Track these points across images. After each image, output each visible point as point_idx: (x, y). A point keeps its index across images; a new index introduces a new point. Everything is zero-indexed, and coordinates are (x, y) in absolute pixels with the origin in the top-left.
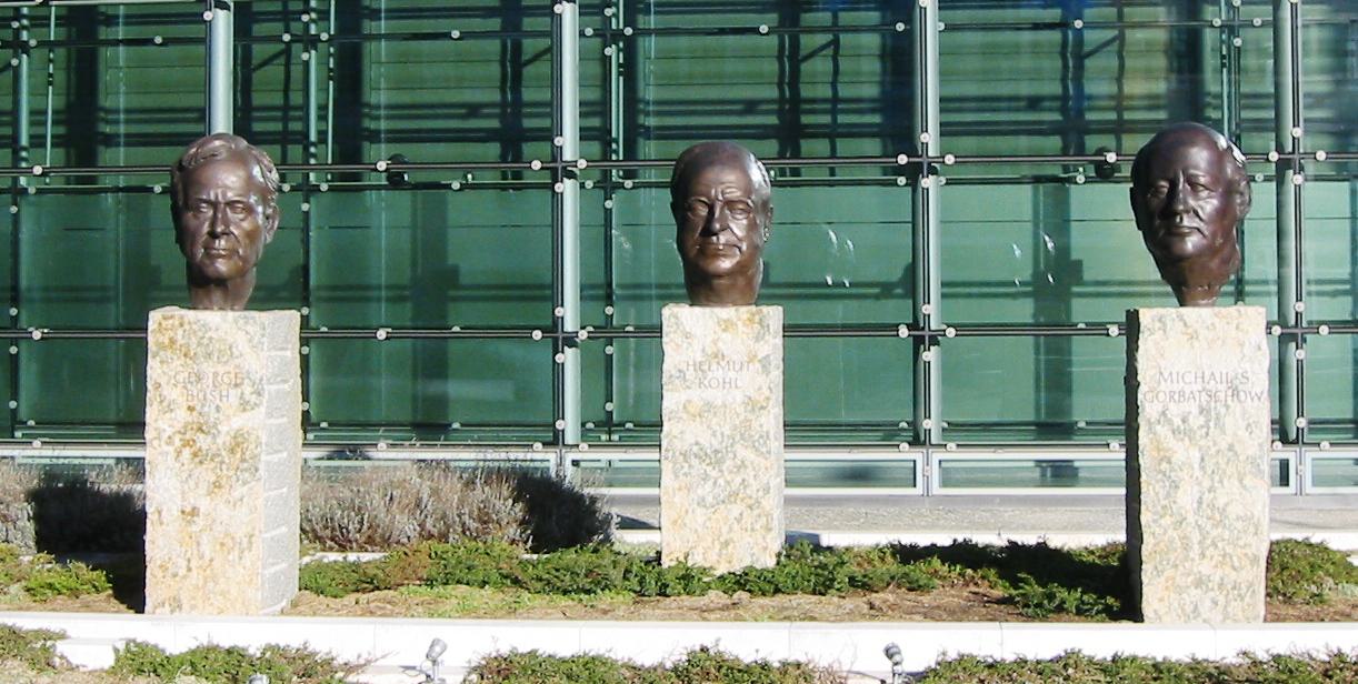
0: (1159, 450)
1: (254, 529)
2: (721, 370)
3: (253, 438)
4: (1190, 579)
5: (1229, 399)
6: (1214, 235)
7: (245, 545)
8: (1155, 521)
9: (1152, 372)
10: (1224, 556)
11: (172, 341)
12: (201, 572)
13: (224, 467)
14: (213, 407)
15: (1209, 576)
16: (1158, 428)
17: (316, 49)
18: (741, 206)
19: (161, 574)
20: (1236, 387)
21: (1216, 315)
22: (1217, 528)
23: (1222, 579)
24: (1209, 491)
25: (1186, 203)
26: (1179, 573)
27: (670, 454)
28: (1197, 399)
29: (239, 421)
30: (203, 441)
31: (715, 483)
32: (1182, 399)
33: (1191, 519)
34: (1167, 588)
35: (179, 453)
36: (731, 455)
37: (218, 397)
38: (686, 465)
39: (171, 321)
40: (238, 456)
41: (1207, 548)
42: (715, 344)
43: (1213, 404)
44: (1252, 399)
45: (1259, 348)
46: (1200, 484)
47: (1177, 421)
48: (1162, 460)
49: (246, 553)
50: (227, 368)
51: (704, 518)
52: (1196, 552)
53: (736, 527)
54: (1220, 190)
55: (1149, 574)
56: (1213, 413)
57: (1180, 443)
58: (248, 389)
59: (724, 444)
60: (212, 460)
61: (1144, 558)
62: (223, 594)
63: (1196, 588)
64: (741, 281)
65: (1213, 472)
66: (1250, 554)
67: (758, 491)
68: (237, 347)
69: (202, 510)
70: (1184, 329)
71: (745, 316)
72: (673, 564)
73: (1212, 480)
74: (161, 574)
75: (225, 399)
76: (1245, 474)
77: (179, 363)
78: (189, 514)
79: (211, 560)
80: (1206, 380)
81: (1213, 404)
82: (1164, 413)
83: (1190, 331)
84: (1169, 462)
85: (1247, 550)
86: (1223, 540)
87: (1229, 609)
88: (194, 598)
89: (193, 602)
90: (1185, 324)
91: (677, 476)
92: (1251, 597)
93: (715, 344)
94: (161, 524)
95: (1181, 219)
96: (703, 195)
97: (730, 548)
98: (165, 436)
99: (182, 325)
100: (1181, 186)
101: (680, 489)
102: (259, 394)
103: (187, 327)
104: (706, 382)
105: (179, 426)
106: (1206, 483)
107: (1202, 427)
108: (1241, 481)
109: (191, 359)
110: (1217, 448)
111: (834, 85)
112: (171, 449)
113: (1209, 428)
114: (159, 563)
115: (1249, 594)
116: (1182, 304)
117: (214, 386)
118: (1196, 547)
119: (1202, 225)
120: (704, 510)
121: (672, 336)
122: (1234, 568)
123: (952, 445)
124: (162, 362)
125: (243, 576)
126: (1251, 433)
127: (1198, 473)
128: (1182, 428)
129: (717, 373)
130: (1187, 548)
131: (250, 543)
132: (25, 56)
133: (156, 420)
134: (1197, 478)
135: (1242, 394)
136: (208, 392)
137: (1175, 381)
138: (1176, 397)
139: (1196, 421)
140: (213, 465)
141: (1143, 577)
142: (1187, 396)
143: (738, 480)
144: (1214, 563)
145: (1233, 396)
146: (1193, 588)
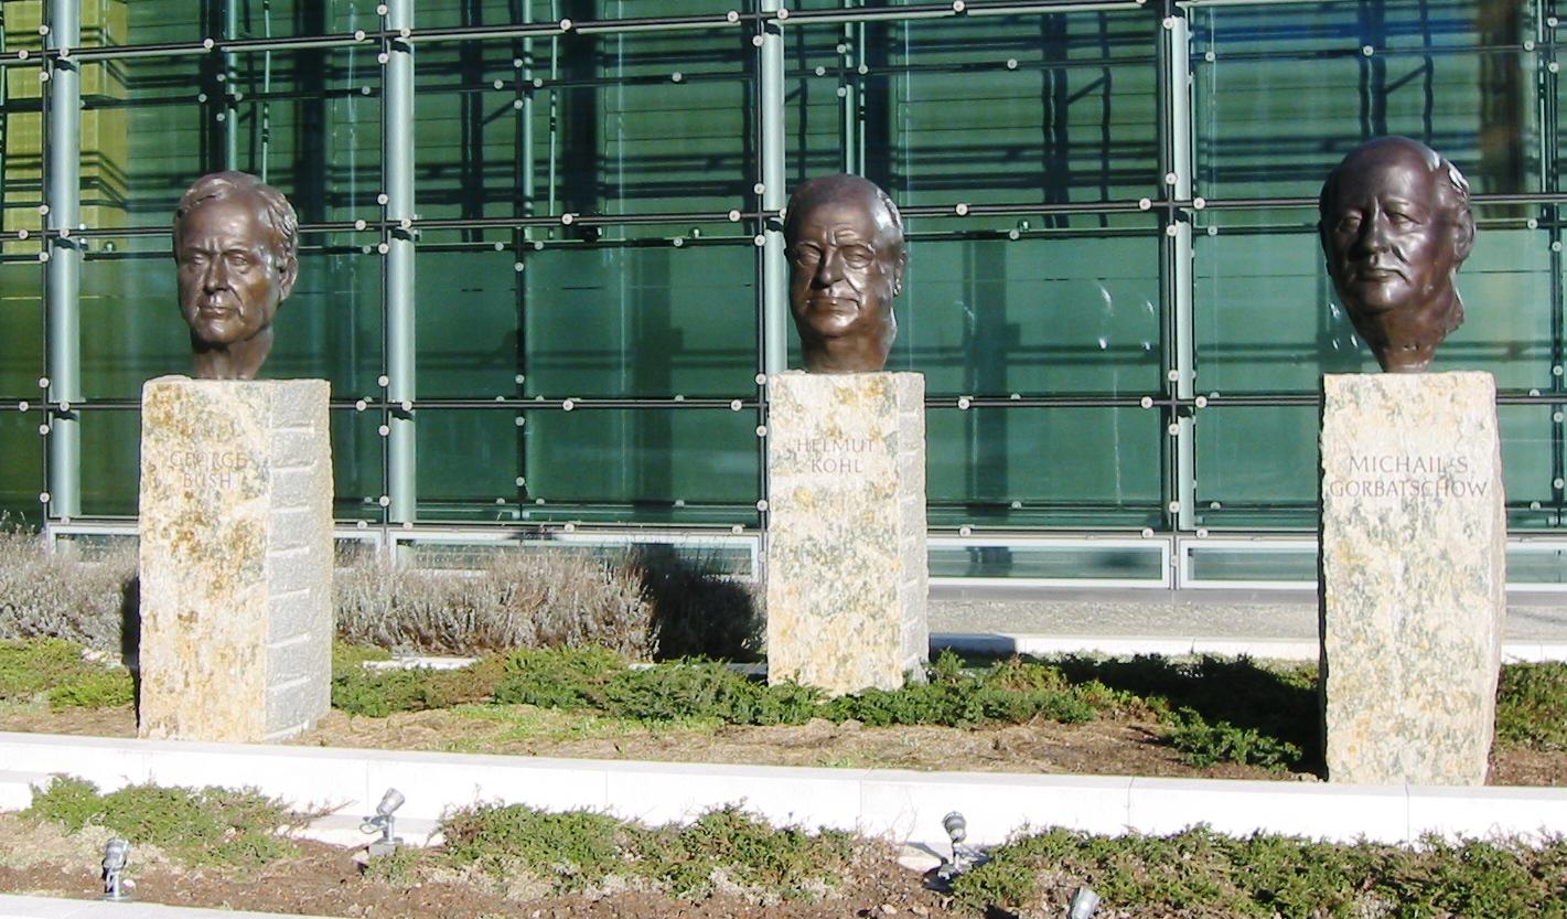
0: (1349, 558)
1: (257, 638)
2: (838, 451)
3: (256, 531)
4: (1390, 723)
5: (1442, 492)
6: (1420, 280)
7: (248, 656)
9: (1340, 457)
10: (1434, 695)
11: (169, 416)
12: (201, 687)
13: (225, 564)
14: (213, 494)
15: (1414, 721)
16: (1349, 528)
17: (531, 97)
18: (859, 252)
19: (157, 689)
20: (1451, 477)
23: (1432, 725)
25: (1381, 238)
27: (779, 550)
28: (1400, 492)
29: (240, 511)
30: (202, 534)
31: (831, 586)
32: (1380, 491)
33: (1391, 646)
34: (1359, 734)
35: (175, 547)
36: (850, 552)
37: (218, 481)
38: (798, 564)
39: (167, 393)
40: (241, 551)
41: (1412, 684)
42: (832, 419)
43: (1420, 499)
44: (1473, 493)
45: (1482, 427)
47: (1373, 521)
48: (1353, 569)
49: (250, 665)
50: (228, 448)
51: (819, 628)
53: (855, 638)
54: (1429, 221)
55: (1335, 716)
56: (1420, 510)
57: (1377, 548)
58: (251, 473)
59: (842, 540)
60: (212, 556)
62: (224, 714)
64: (863, 343)
65: (1420, 586)
67: (882, 596)
68: (239, 424)
69: (201, 615)
70: (1383, 403)
71: (867, 385)
72: (782, 682)
73: (1419, 596)
74: (157, 689)
75: (226, 484)
77: (176, 441)
78: (185, 620)
79: (211, 674)
80: (1411, 469)
81: (1420, 499)
82: (1356, 510)
83: (1390, 403)
84: (1363, 573)
85: (1466, 689)
86: (1434, 674)
87: (1441, 763)
88: (191, 719)
89: (191, 723)
90: (1384, 395)
91: (786, 578)
93: (832, 419)
94: (157, 630)
95: (1377, 260)
96: (810, 239)
97: (849, 664)
98: (161, 527)
99: (178, 397)
100: (1376, 217)
101: (790, 593)
102: (263, 478)
103: (184, 399)
104: (821, 465)
105: (175, 516)
106: (1412, 601)
107: (1406, 528)
108: (1457, 598)
109: (188, 436)
110: (1425, 555)
111: (1105, 126)
112: (166, 543)
113: (1414, 530)
114: (153, 676)
116: (1385, 369)
117: (214, 469)
118: (1397, 682)
119: (1405, 269)
120: (819, 618)
121: (780, 409)
122: (1448, 711)
123: (1203, 531)
124: (157, 441)
125: (246, 694)
126: (1470, 537)
127: (1400, 587)
128: (1380, 528)
129: (833, 453)
130: (1385, 683)
131: (254, 655)
132: (232, 111)
133: (151, 509)
135: (1458, 485)
136: (207, 476)
137: (1370, 468)
138: (1372, 489)
139: (1398, 520)
140: (212, 562)
141: (1328, 720)
143: (859, 583)
144: (1420, 703)
145: (1447, 487)
146: (1393, 735)
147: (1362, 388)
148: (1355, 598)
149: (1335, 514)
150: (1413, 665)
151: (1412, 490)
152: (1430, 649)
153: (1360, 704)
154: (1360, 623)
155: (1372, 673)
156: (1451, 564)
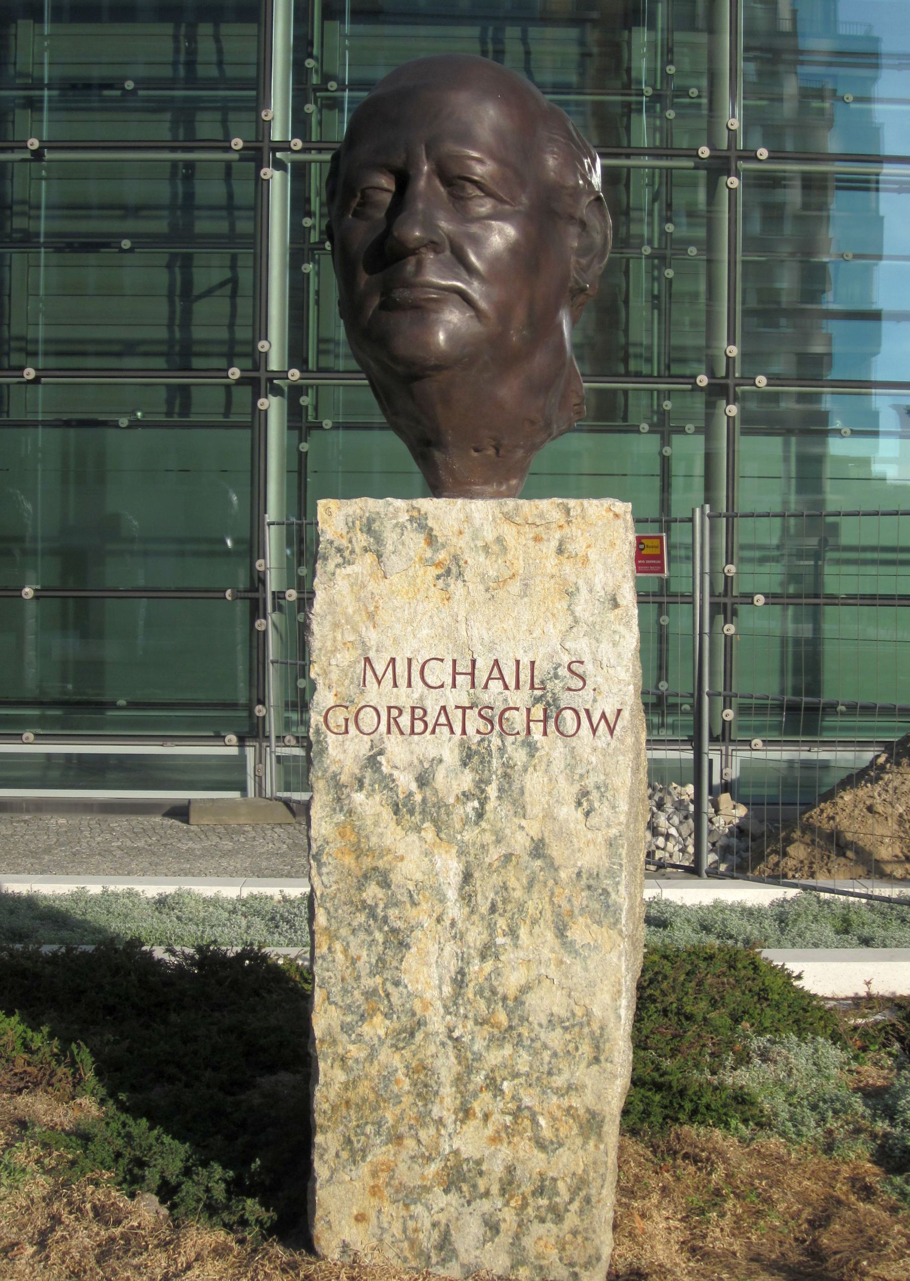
0: (358, 851)
4: (433, 1168)
5: (537, 728)
6: (504, 312)
8: (346, 1028)
10: (516, 1114)
16: (359, 797)
21: (508, 518)
22: (501, 1047)
23: (510, 1170)
24: (483, 957)
25: (429, 225)
26: (404, 1155)
28: (458, 729)
32: (419, 726)
33: (437, 1023)
41: (475, 1095)
43: (495, 741)
45: (616, 605)
46: (459, 937)
47: (406, 782)
52: (448, 1101)
55: (330, 1156)
56: (495, 763)
57: (413, 837)
61: (319, 1119)
63: (446, 1191)
65: (493, 909)
66: (581, 1111)
70: (429, 554)
73: (491, 928)
76: (571, 914)
81: (495, 741)
82: (372, 762)
83: (442, 555)
84: (385, 884)
85: (575, 1101)
86: (516, 1075)
87: (527, 1242)
90: (431, 540)
92: (581, 1212)
95: (420, 265)
100: (422, 183)
106: (476, 936)
108: (561, 931)
110: (503, 851)
115: (575, 1206)
118: (447, 1091)
122: (541, 1145)
126: (587, 814)
127: (455, 910)
128: (418, 798)
134: (453, 924)
135: (568, 715)
137: (402, 681)
138: (405, 721)
141: (317, 1164)
142: (431, 720)
144: (490, 1131)
146: (438, 1190)
147: (389, 525)
148: (369, 932)
149: (334, 768)
150: (478, 1058)
151: (481, 724)
152: (511, 1028)
153: (378, 1133)
154: (378, 979)
155: (400, 1075)
156: (552, 866)
